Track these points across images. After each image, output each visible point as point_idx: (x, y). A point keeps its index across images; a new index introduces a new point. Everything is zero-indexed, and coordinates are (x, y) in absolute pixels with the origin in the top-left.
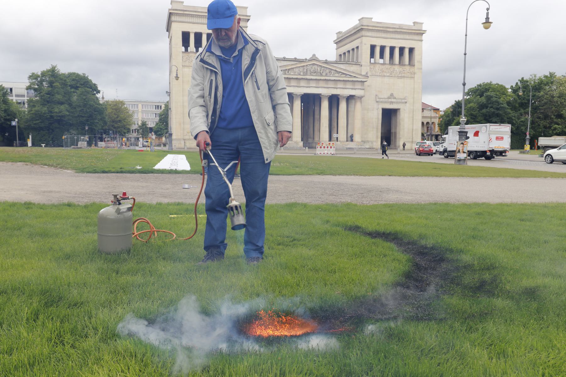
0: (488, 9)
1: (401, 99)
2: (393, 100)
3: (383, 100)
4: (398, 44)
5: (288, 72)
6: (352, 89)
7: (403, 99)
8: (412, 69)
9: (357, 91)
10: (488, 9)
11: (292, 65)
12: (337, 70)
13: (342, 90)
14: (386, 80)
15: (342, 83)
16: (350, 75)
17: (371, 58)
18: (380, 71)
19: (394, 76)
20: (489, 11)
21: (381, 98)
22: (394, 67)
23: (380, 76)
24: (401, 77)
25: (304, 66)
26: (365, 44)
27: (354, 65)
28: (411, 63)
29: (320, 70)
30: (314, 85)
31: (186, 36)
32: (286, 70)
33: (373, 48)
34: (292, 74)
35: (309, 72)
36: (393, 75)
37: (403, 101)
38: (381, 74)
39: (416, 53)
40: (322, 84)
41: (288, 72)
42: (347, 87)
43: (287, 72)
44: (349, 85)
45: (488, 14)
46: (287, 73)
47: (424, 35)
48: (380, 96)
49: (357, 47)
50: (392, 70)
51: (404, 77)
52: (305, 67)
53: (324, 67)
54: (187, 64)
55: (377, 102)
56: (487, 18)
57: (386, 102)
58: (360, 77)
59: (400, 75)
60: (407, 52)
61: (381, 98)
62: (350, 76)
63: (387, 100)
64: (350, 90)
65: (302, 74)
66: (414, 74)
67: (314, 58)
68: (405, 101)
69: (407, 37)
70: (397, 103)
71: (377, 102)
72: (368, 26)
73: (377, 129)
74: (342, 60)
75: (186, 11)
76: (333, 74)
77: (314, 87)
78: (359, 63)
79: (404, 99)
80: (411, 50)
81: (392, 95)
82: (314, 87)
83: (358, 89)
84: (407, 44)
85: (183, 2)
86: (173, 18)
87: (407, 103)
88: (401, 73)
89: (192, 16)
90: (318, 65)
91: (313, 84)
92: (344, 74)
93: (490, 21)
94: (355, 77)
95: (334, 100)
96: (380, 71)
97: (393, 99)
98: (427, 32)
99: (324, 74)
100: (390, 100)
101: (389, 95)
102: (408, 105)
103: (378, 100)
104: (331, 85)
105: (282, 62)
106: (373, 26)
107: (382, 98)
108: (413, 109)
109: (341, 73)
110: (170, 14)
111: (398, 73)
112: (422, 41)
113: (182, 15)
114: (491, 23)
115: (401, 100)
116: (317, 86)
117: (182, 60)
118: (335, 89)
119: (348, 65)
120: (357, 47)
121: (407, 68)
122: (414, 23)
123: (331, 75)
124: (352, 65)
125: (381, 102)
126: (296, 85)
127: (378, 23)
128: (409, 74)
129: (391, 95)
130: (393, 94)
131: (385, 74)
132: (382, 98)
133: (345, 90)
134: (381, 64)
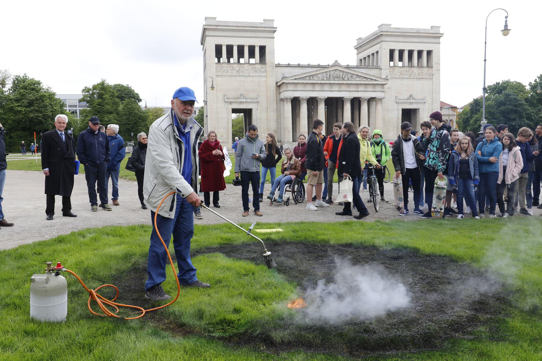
0: (506, 17)
1: (420, 100)
2: (412, 101)
3: (403, 101)
4: (416, 47)
5: (313, 78)
6: (373, 91)
7: (422, 100)
8: (430, 71)
9: (377, 93)
10: (506, 17)
12: (359, 74)
13: (363, 93)
14: (405, 82)
15: (363, 86)
16: (370, 79)
17: (390, 61)
18: (399, 74)
19: (413, 78)
20: (507, 19)
21: (400, 100)
22: (412, 69)
23: (399, 78)
24: (420, 78)
25: (327, 72)
27: (374, 69)
28: (429, 65)
29: (343, 75)
30: (337, 89)
31: (218, 50)
32: (311, 75)
33: (392, 52)
34: (316, 79)
37: (422, 101)
38: (400, 77)
39: (434, 55)
40: (344, 88)
41: (313, 78)
42: (368, 90)
43: (311, 78)
44: (370, 88)
45: (506, 22)
46: (311, 79)
47: (441, 37)
48: (400, 98)
49: (377, 52)
50: (411, 72)
51: (422, 78)
52: (328, 73)
53: (346, 72)
54: (220, 74)
55: (397, 103)
56: (506, 26)
57: (405, 103)
58: (381, 80)
59: (419, 77)
60: (425, 54)
61: (400, 100)
62: (370, 80)
63: (407, 101)
64: (372, 93)
65: (325, 79)
67: (336, 64)
68: (424, 101)
69: (425, 40)
70: (416, 103)
71: (397, 103)
72: (387, 32)
73: (398, 128)
74: (363, 65)
75: (218, 26)
76: (354, 78)
77: (337, 91)
78: (379, 67)
79: (423, 99)
80: (429, 53)
81: (411, 96)
82: (337, 91)
83: (379, 91)
84: (425, 48)
85: (215, 18)
86: (207, 33)
87: (426, 103)
88: (420, 74)
89: (224, 30)
90: (340, 70)
91: (336, 88)
92: (365, 78)
93: (508, 28)
95: (356, 103)
96: (399, 74)
97: (413, 99)
98: (444, 35)
99: (346, 79)
100: (409, 101)
101: (408, 96)
102: (426, 105)
103: (397, 101)
104: (353, 88)
105: (307, 68)
106: (392, 32)
107: (402, 100)
108: (432, 109)
109: (362, 77)
110: (205, 30)
111: (417, 75)
112: (439, 43)
113: (215, 30)
114: (509, 30)
115: (420, 101)
116: (340, 89)
117: (216, 71)
118: (357, 92)
119: (368, 69)
120: (377, 52)
121: (426, 70)
122: (432, 27)
123: (353, 80)
124: (372, 69)
125: (401, 103)
126: (320, 90)
127: (396, 28)
128: (427, 75)
129: (410, 96)
130: (412, 95)
131: (404, 77)
132: (402, 100)
133: (366, 93)
134: (400, 67)
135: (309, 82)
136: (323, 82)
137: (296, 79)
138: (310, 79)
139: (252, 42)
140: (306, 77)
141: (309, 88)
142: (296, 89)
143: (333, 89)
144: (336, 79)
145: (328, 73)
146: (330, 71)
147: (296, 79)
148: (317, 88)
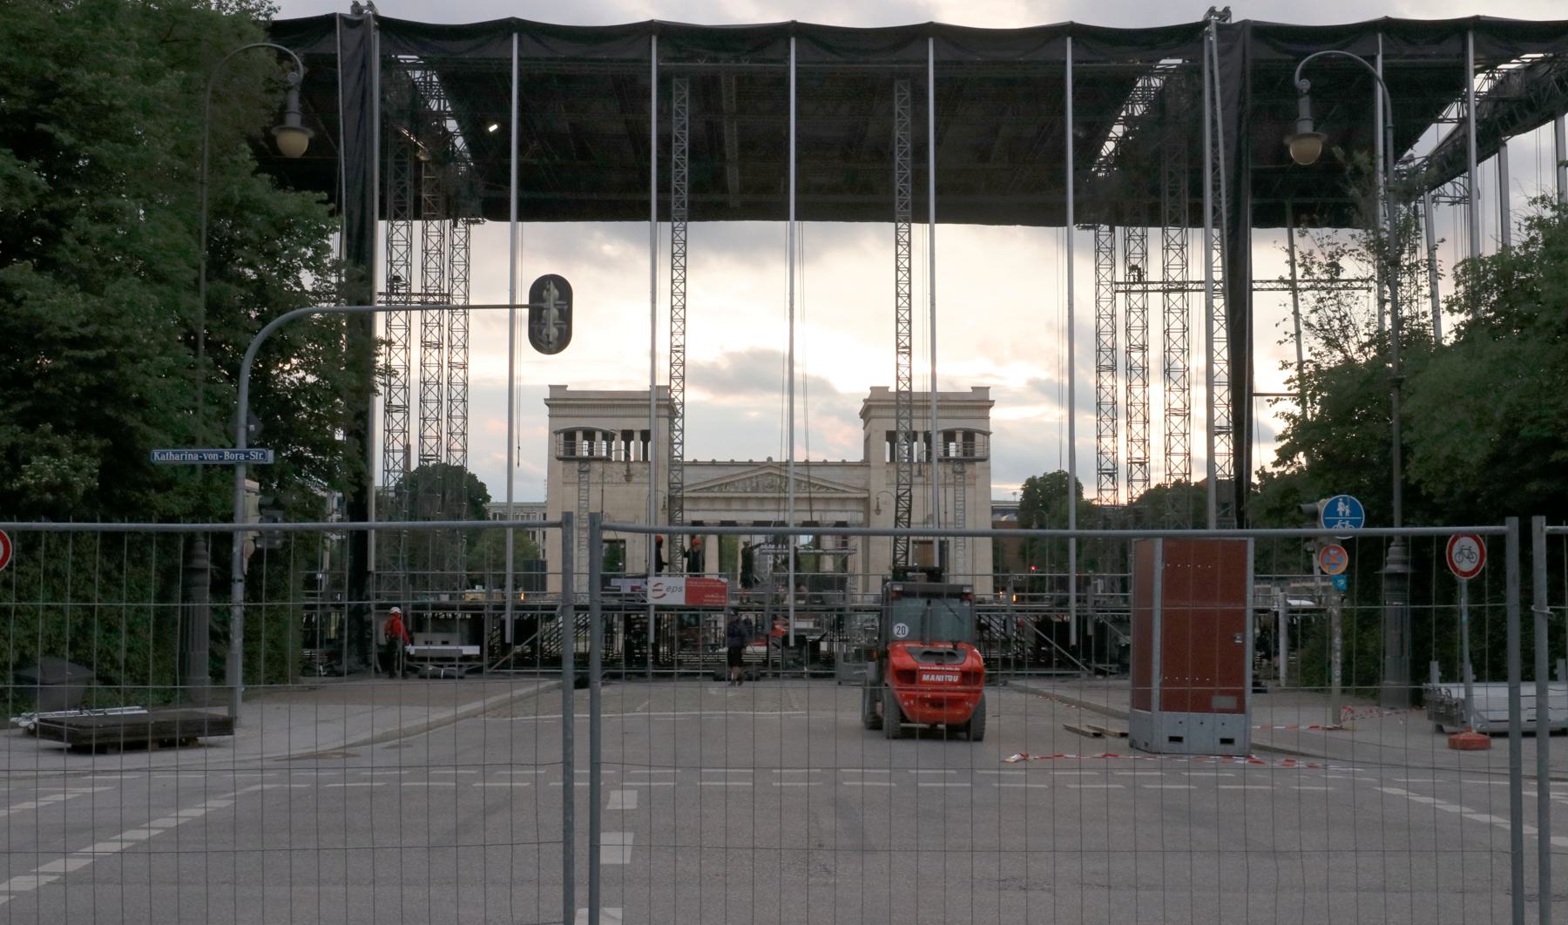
6: (841, 511)
11: (746, 473)
35: (761, 486)
42: (832, 508)
65: (749, 490)
66: (975, 478)
67: (770, 463)
69: (959, 413)
72: (879, 401)
80: (969, 436)
94: (843, 491)
105: (729, 468)
135: (718, 495)
136: (744, 495)
137: (694, 491)
138: (721, 491)
139: (628, 424)
140: (714, 486)
141: (720, 505)
142: (695, 508)
143: (765, 508)
144: (770, 490)
146: (757, 476)
147: (694, 491)
148: (735, 505)
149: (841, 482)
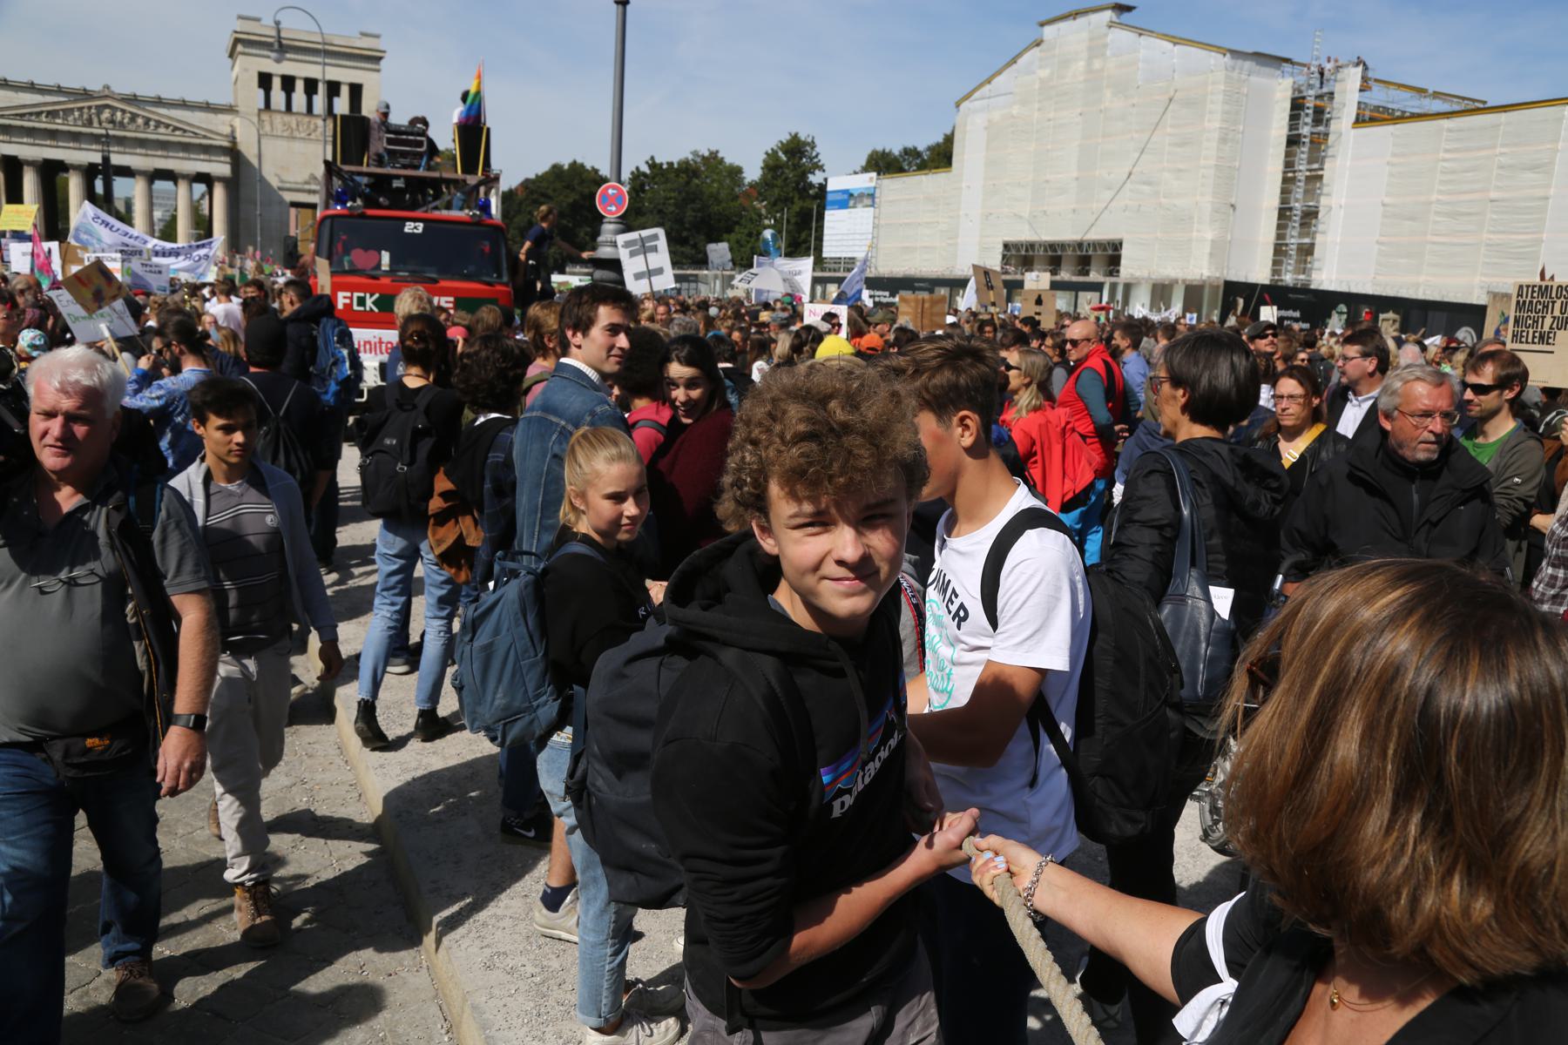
26: (246, 70)
32: (42, 112)
36: (312, 137)
48: (285, 178)
67: (106, 92)
92: (176, 129)
94: (205, 137)
101: (306, 177)
135: (37, 125)
140: (31, 114)
145: (86, 111)
146: (90, 108)
149: (204, 126)
